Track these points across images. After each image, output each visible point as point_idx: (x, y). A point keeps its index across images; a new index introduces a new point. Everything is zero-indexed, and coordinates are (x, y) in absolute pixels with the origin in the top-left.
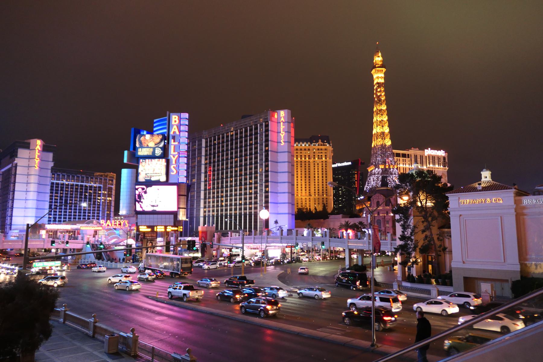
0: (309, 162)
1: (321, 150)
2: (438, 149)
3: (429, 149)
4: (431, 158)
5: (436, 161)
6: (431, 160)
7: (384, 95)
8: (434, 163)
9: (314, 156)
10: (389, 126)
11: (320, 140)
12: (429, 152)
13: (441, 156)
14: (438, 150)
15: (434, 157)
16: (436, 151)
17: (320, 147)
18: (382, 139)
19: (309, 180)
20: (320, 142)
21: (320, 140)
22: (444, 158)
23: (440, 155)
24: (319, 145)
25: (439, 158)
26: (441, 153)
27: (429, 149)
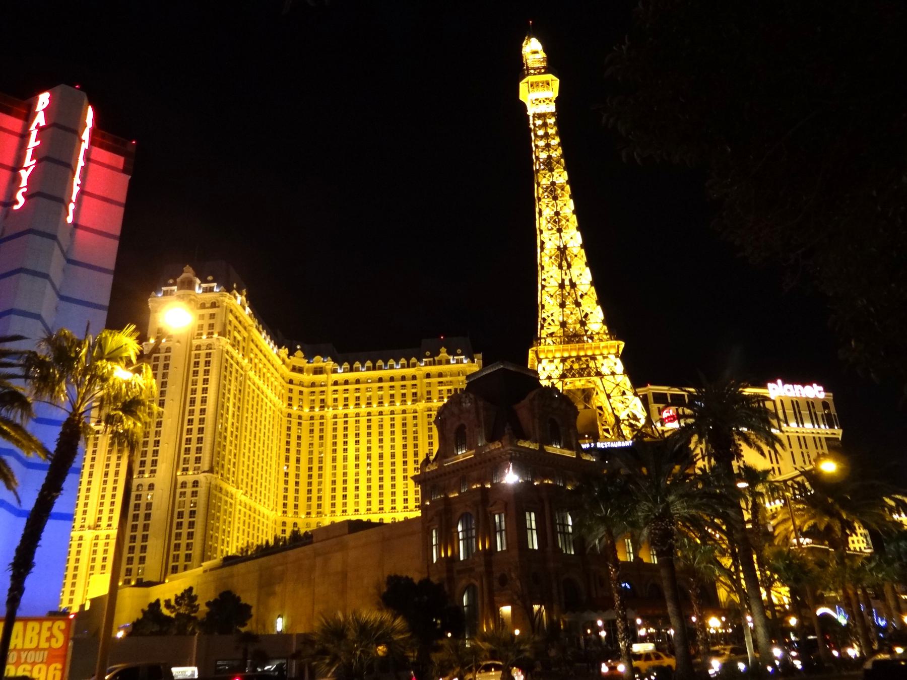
2: (805, 381)
3: (779, 381)
5: (805, 413)
7: (559, 144)
8: (800, 420)
9: (429, 393)
10: (580, 228)
11: (443, 350)
13: (816, 399)
14: (804, 385)
15: (795, 404)
16: (798, 387)
20: (443, 354)
21: (443, 350)
22: (825, 405)
25: (811, 404)
26: (815, 392)
27: (779, 381)
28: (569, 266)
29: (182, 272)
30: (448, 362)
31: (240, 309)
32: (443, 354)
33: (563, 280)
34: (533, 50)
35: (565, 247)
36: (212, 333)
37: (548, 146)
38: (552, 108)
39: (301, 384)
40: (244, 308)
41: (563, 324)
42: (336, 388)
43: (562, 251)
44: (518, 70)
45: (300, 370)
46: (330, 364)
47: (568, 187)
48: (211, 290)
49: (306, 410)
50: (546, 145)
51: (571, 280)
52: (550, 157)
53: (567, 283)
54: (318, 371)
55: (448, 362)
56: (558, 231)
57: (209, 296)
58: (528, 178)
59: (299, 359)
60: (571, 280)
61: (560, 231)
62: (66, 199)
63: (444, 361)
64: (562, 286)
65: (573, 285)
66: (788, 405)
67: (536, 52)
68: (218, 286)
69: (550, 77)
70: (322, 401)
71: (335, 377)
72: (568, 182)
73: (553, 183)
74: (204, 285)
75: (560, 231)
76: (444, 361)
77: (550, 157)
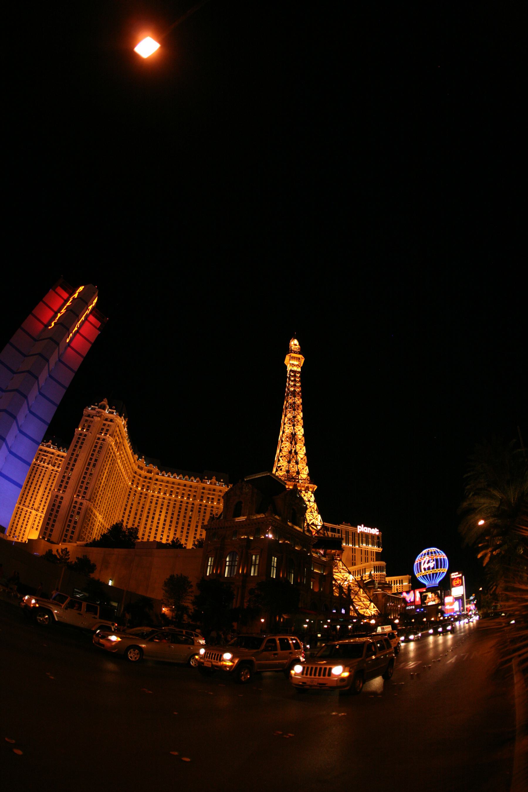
0: (193, 504)
1: (214, 490)
2: (372, 527)
3: (363, 525)
4: (364, 536)
6: (364, 539)
7: (300, 386)
8: (367, 543)
9: (202, 497)
11: (214, 477)
12: (361, 529)
13: (375, 534)
16: (369, 529)
17: (213, 487)
18: (291, 443)
19: (188, 529)
20: (214, 480)
22: (378, 537)
23: (374, 533)
24: (211, 483)
25: (373, 536)
26: (375, 531)
27: (363, 525)
28: (296, 444)
29: (102, 401)
30: (215, 484)
31: (123, 427)
32: (214, 480)
33: (291, 450)
34: (294, 344)
35: (295, 433)
36: (107, 434)
37: (295, 385)
38: (299, 370)
39: (140, 475)
40: (124, 428)
41: (288, 471)
42: (156, 482)
43: (293, 436)
44: (287, 350)
45: (141, 468)
46: (155, 469)
47: (301, 407)
48: (112, 413)
49: (139, 489)
50: (293, 385)
51: (295, 451)
52: (295, 390)
53: (293, 451)
54: (150, 472)
55: (215, 484)
56: (292, 427)
57: (111, 415)
58: (282, 398)
59: (142, 462)
60: (295, 451)
61: (294, 425)
62: (80, 317)
63: (213, 483)
64: (290, 452)
65: (296, 453)
66: (364, 536)
67: (296, 345)
68: (116, 412)
69: (300, 356)
70: (148, 487)
71: (157, 477)
72: (301, 404)
73: (294, 403)
74: (110, 410)
75: (294, 425)
76: (213, 483)
77: (295, 390)
